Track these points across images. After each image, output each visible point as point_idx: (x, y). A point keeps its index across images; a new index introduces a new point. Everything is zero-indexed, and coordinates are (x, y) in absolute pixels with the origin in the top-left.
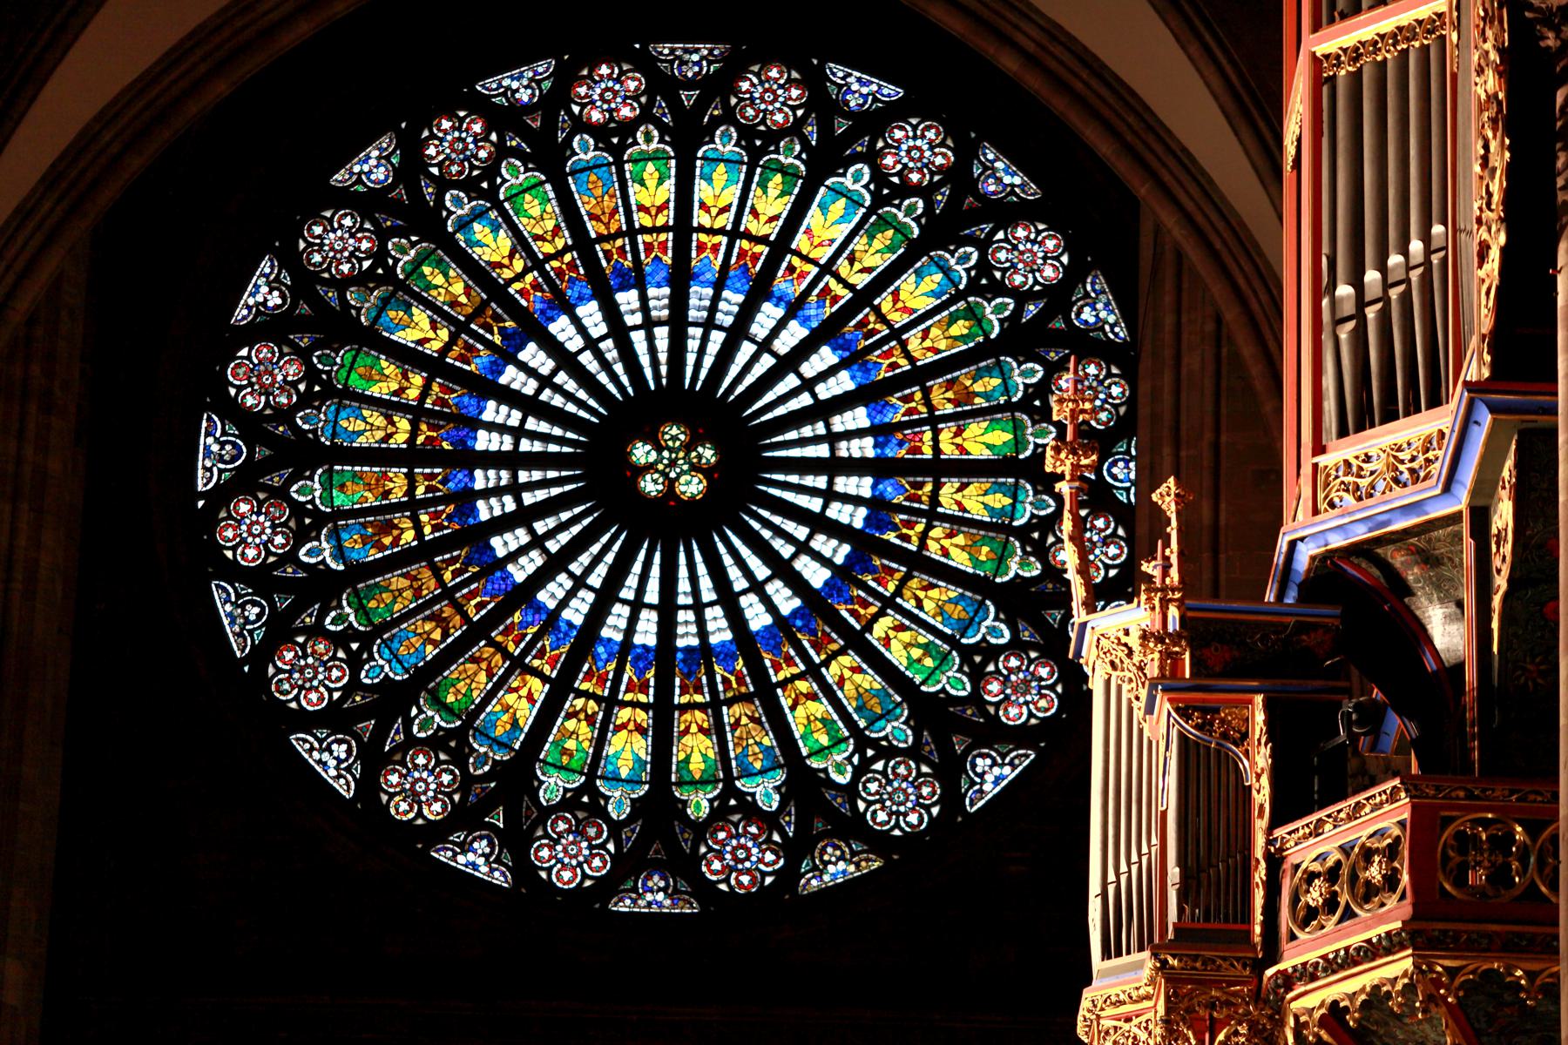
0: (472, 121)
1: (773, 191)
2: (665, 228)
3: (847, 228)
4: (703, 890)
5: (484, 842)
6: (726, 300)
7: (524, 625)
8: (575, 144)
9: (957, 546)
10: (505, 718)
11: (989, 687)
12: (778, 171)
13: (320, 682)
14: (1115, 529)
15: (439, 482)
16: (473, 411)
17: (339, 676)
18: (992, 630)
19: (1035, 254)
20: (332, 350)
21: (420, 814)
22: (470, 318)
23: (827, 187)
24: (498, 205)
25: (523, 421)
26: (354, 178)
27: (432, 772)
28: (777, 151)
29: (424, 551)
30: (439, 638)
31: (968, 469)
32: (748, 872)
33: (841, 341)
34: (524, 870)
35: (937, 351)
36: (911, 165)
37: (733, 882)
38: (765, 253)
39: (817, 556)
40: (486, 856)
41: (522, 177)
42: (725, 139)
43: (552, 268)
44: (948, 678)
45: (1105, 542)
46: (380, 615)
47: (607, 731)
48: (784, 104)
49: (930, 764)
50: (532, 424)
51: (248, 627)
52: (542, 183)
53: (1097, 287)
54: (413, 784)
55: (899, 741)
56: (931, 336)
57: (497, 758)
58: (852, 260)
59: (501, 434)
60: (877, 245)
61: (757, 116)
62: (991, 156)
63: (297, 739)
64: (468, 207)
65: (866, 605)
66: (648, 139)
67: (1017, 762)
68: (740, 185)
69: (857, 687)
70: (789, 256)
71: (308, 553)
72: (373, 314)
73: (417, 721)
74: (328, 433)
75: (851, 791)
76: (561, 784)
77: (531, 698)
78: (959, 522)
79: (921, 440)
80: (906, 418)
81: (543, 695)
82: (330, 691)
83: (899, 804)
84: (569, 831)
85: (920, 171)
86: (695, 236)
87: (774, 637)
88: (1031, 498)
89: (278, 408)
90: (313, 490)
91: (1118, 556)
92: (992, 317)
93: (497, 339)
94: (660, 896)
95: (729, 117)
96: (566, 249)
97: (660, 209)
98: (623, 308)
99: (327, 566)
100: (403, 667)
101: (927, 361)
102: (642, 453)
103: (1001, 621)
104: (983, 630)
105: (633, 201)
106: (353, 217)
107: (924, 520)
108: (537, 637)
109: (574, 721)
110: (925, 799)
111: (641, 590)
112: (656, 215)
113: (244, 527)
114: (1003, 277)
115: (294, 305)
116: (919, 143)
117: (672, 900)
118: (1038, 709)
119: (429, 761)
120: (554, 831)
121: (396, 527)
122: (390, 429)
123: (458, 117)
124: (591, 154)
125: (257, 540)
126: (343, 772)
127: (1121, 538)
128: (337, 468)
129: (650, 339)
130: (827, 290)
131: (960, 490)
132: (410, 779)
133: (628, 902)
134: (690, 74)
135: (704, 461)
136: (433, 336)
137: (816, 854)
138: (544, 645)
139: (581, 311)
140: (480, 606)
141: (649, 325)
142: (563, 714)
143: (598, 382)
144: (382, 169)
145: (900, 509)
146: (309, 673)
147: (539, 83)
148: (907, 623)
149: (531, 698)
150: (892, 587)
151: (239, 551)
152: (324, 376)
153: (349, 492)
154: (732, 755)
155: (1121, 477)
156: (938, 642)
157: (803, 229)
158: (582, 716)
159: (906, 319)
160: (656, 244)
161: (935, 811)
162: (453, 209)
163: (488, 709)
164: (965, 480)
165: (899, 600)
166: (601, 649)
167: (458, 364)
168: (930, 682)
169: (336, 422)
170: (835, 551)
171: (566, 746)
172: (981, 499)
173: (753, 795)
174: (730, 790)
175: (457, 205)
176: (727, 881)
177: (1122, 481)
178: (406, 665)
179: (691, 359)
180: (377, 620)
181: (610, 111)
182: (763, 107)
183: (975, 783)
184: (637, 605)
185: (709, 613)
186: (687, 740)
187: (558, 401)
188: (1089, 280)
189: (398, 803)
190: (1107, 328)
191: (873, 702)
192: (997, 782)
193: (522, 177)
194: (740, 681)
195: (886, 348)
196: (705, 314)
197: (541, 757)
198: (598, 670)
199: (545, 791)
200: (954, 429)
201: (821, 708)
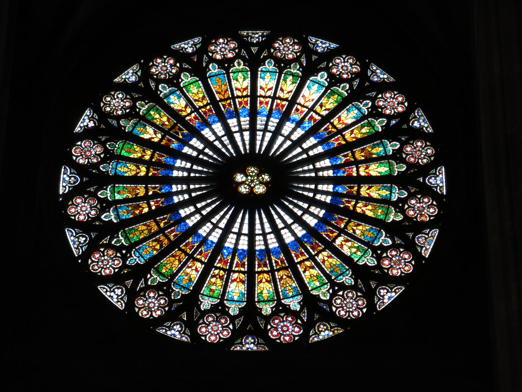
0: (169, 59)
2: (247, 96)
3: (319, 95)
5: (179, 326)
6: (272, 121)
9: (368, 210)
10: (186, 278)
11: (384, 262)
12: (291, 75)
13: (110, 266)
15: (159, 190)
17: (119, 264)
18: (384, 241)
19: (394, 103)
20: (114, 142)
21: (151, 315)
22: (170, 129)
23: (310, 80)
24: (181, 89)
26: (123, 80)
28: (290, 68)
29: (152, 215)
30: (159, 248)
31: (371, 180)
32: (288, 335)
33: (318, 135)
34: (195, 336)
36: (343, 72)
37: (282, 340)
38: (287, 104)
40: (180, 332)
42: (270, 64)
43: (202, 111)
44: (367, 259)
45: (429, 207)
47: (228, 282)
48: (292, 51)
50: (195, 167)
52: (197, 81)
54: (149, 304)
56: (354, 133)
57: (183, 293)
58: (321, 106)
59: (183, 172)
60: (331, 100)
61: (282, 56)
62: (375, 68)
63: (101, 288)
65: (332, 232)
66: (239, 64)
67: (397, 291)
68: (276, 80)
72: (131, 129)
73: (150, 280)
75: (329, 303)
77: (196, 270)
78: (369, 200)
79: (352, 171)
81: (202, 269)
82: (114, 269)
83: (349, 308)
84: (213, 321)
85: (347, 74)
88: (397, 191)
91: (434, 212)
92: (378, 125)
93: (181, 137)
95: (271, 56)
96: (208, 104)
97: (244, 89)
98: (231, 125)
100: (144, 259)
102: (239, 178)
103: (388, 237)
104: (381, 241)
106: (122, 94)
107: (355, 200)
108: (199, 247)
109: (215, 278)
110: (360, 306)
111: (241, 228)
112: (243, 92)
113: (79, 208)
114: (382, 111)
116: (346, 64)
117: (257, 347)
119: (155, 295)
120: (207, 321)
121: (141, 207)
122: (138, 171)
124: (217, 70)
125: (84, 213)
127: (435, 205)
128: (117, 185)
129: (242, 136)
130: (311, 117)
131: (368, 189)
135: (265, 180)
136: (155, 136)
137: (316, 328)
138: (202, 250)
139: (214, 126)
141: (241, 131)
142: (210, 276)
144: (134, 77)
146: (105, 262)
148: (350, 239)
149: (196, 270)
150: (342, 226)
153: (122, 194)
154: (280, 290)
155: (433, 183)
156: (362, 245)
157: (301, 95)
158: (218, 277)
160: (243, 102)
162: (163, 91)
163: (180, 274)
164: (370, 185)
166: (225, 251)
168: (360, 261)
169: (116, 169)
172: (377, 192)
173: (289, 305)
175: (164, 90)
176: (279, 339)
178: (145, 258)
181: (224, 55)
182: (284, 52)
183: (381, 299)
184: (239, 234)
185: (269, 237)
186: (261, 285)
187: (205, 158)
188: (416, 111)
189: (142, 311)
190: (424, 129)
191: (337, 269)
192: (389, 298)
194: (282, 262)
195: (336, 137)
196: (263, 127)
199: (203, 305)
200: (365, 167)
201: (315, 272)
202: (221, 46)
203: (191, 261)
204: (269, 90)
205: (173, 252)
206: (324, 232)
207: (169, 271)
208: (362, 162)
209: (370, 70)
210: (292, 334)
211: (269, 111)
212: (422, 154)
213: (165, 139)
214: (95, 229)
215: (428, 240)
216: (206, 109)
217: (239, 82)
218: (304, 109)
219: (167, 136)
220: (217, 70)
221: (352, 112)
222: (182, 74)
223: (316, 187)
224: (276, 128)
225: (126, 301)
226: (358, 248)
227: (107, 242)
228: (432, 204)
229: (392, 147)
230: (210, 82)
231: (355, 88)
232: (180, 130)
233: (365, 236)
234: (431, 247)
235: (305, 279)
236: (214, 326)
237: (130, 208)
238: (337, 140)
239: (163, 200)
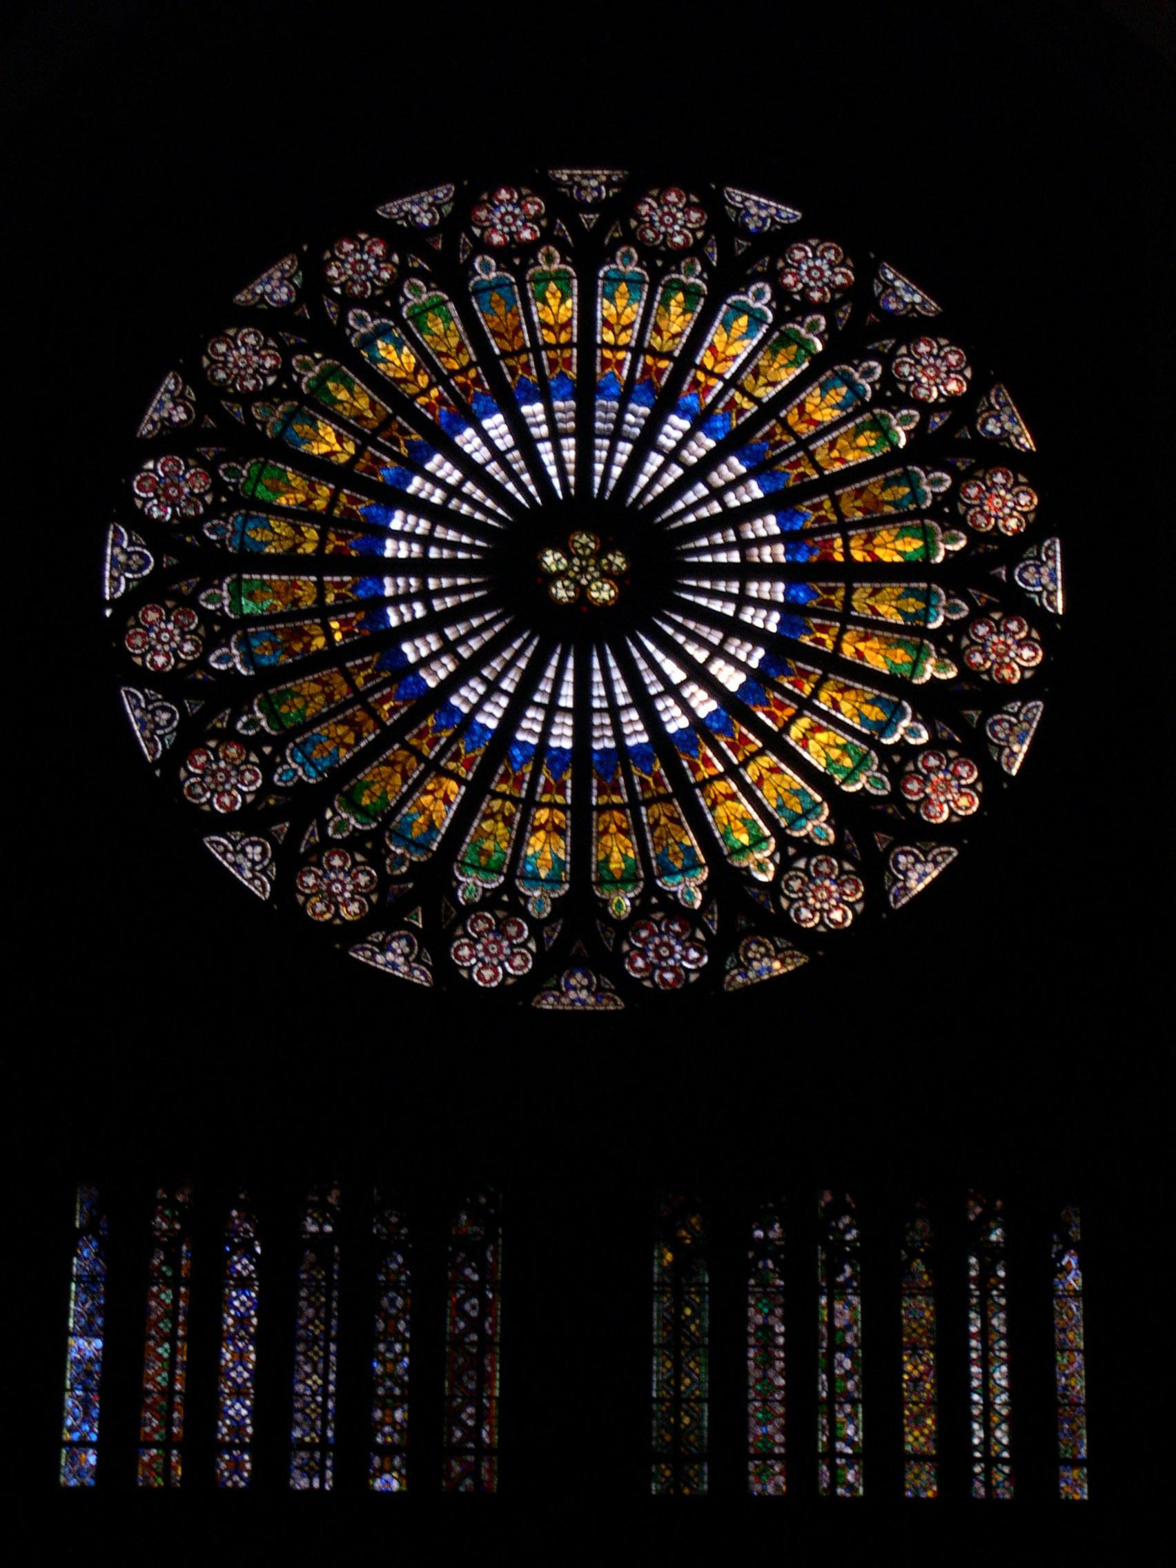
0: (374, 244)
2: (569, 345)
4: (627, 987)
7: (438, 729)
8: (477, 266)
9: (871, 649)
10: (421, 820)
14: (1029, 633)
15: (351, 590)
16: (382, 523)
17: (252, 783)
18: (910, 731)
21: (337, 914)
22: (376, 432)
24: (401, 323)
25: (432, 530)
26: (257, 298)
27: (348, 874)
28: (678, 271)
29: (333, 656)
32: (672, 969)
33: (747, 452)
34: (445, 969)
37: (657, 979)
40: (406, 956)
41: (424, 296)
42: (626, 260)
45: (1020, 644)
46: (292, 720)
49: (852, 862)
50: (439, 532)
51: (159, 732)
52: (444, 302)
53: (1001, 400)
56: (838, 446)
57: (414, 859)
58: (756, 373)
59: (409, 543)
60: (781, 359)
63: (211, 842)
64: (371, 325)
65: (782, 706)
66: (550, 259)
67: (939, 859)
68: (643, 304)
71: (219, 660)
72: (279, 429)
73: (332, 824)
74: (237, 542)
76: (479, 883)
77: (447, 801)
84: (489, 930)
85: (821, 290)
86: (599, 352)
88: (944, 603)
89: (184, 519)
90: (221, 598)
91: (1033, 658)
93: (404, 451)
94: (584, 994)
95: (630, 238)
96: (471, 365)
98: (530, 420)
99: (238, 672)
102: (551, 560)
104: (901, 731)
105: (536, 319)
106: (256, 335)
108: (451, 740)
113: (153, 635)
114: (908, 389)
115: (200, 419)
116: (818, 263)
119: (345, 862)
120: (473, 930)
121: (307, 634)
122: (298, 539)
123: (360, 240)
124: (493, 275)
128: (246, 576)
129: (557, 450)
130: (732, 402)
131: (872, 595)
132: (325, 880)
133: (551, 999)
134: (589, 199)
135: (615, 568)
137: (741, 951)
138: (459, 749)
139: (486, 423)
140: (393, 711)
141: (555, 437)
142: (479, 815)
143: (508, 492)
144: (285, 290)
146: (221, 777)
147: (439, 207)
148: (824, 724)
149: (447, 801)
150: (808, 689)
151: (148, 657)
152: (231, 488)
154: (652, 854)
155: (1033, 581)
156: (856, 742)
157: (706, 345)
158: (499, 817)
160: (560, 360)
162: (356, 327)
163: (405, 810)
166: (516, 752)
169: (243, 533)
170: (749, 655)
172: (894, 603)
173: (675, 893)
174: (651, 888)
175: (360, 322)
176: (651, 978)
177: (1033, 586)
180: (289, 724)
181: (511, 233)
182: (663, 229)
184: (552, 709)
186: (608, 840)
187: (465, 509)
188: (993, 393)
190: (1013, 439)
193: (424, 296)
194: (658, 780)
195: (793, 458)
196: (611, 426)
198: (514, 771)
200: (864, 537)
202: (503, 210)
206: (762, 704)
208: (856, 525)
211: (624, 387)
214: (196, 690)
215: (1016, 729)
216: (467, 377)
218: (712, 382)
219: (370, 448)
223: (743, 588)
224: (644, 429)
226: (843, 748)
230: (476, 306)
232: (404, 432)
235: (713, 827)
239: (362, 615)
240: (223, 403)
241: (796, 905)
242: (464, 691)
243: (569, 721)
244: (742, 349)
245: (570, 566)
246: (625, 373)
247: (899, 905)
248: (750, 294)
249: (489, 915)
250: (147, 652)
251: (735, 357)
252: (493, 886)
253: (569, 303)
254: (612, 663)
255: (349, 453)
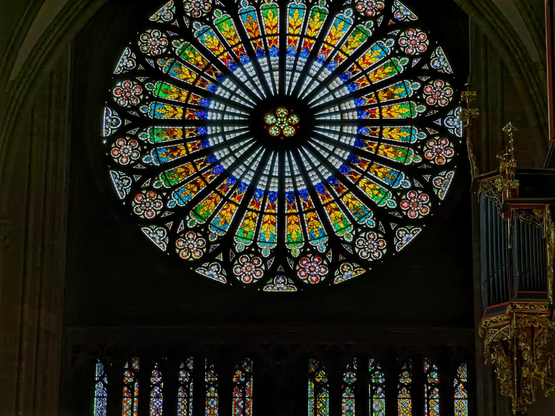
1: (316, 20)
2: (276, 34)
3: (344, 33)
5: (216, 266)
9: (390, 152)
10: (222, 220)
11: (403, 205)
12: (318, 12)
13: (152, 208)
14: (449, 144)
16: (206, 105)
17: (159, 205)
18: (404, 183)
19: (416, 41)
21: (191, 257)
22: (204, 70)
23: (337, 17)
24: (213, 27)
25: (225, 108)
26: (159, 18)
29: (190, 158)
30: (196, 190)
31: (393, 122)
32: (315, 275)
34: (231, 277)
35: (380, 79)
36: (368, 8)
37: (309, 280)
38: (314, 43)
39: (337, 157)
41: (222, 16)
43: (234, 50)
46: (174, 182)
52: (229, 18)
53: (440, 53)
54: (188, 245)
55: (370, 225)
56: (378, 73)
58: (347, 45)
59: (217, 113)
60: (356, 39)
62: (398, 4)
63: (144, 229)
64: (202, 28)
65: (356, 174)
67: (415, 232)
69: (354, 205)
70: (323, 44)
72: (167, 69)
73: (189, 222)
75: (353, 245)
76: (244, 244)
77: (232, 213)
79: (375, 112)
80: (369, 104)
81: (236, 211)
82: (156, 211)
83: (371, 249)
84: (247, 262)
85: (372, 10)
86: (287, 37)
87: (322, 187)
88: (417, 133)
90: (147, 136)
92: (401, 65)
93: (214, 77)
94: (282, 285)
96: (239, 43)
97: (274, 27)
98: (261, 65)
100: (183, 202)
101: (376, 82)
102: (270, 119)
103: (407, 179)
104: (401, 183)
105: (264, 24)
106: (158, 32)
107: (377, 142)
108: (233, 189)
109: (248, 220)
110: (380, 247)
112: (273, 30)
113: (121, 150)
115: (137, 66)
118: (422, 213)
121: (178, 149)
122: (175, 112)
124: (247, 7)
126: (162, 242)
128: (156, 127)
129: (272, 76)
130: (338, 56)
133: (270, 288)
135: (293, 122)
137: (340, 269)
138: (236, 192)
139: (245, 66)
140: (211, 178)
141: (271, 71)
142: (244, 218)
144: (169, 14)
145: (368, 138)
146: (148, 205)
148: (372, 181)
149: (231, 213)
150: (366, 167)
151: (120, 159)
153: (161, 136)
154: (308, 232)
155: (451, 124)
156: (384, 188)
157: (328, 33)
158: (251, 218)
159: (368, 66)
160: (273, 40)
161: (385, 251)
163: (216, 216)
164: (392, 127)
165: (368, 173)
166: (257, 193)
167: (200, 87)
169: (155, 110)
170: (344, 154)
171: (245, 230)
172: (398, 134)
173: (316, 247)
174: (307, 245)
175: (197, 27)
176: (307, 279)
177: (451, 126)
178: (184, 201)
179: (287, 83)
180: (172, 184)
183: (400, 241)
184: (270, 176)
187: (238, 100)
188: (437, 50)
189: (182, 253)
190: (444, 68)
191: (360, 211)
192: (407, 240)
193: (222, 16)
194: (310, 204)
195: (361, 78)
196: (292, 66)
197: (236, 234)
198: (256, 201)
200: (387, 108)
201: (340, 213)
203: (226, 203)
204: (297, 27)
205: (209, 195)
206: (349, 174)
207: (206, 213)
209: (394, 6)
210: (318, 274)
211: (297, 51)
212: (441, 95)
213: (200, 79)
217: (269, 20)
218: (330, 48)
219: (201, 76)
220: (247, 7)
221: (376, 51)
222: (215, 11)
223: (341, 129)
225: (167, 243)
227: (149, 184)
228: (449, 146)
229: (413, 87)
231: (379, 26)
232: (214, 70)
233: (386, 178)
234: (447, 189)
235: (330, 221)
236: (248, 266)
237: (169, 150)
238: (361, 80)
239: (199, 142)
240: (146, 59)
241: (361, 251)
242: (237, 170)
243: (277, 181)
244: (342, 35)
245: (277, 121)
246: (297, 45)
247: (400, 250)
248: (345, 13)
249: (247, 256)
250: (119, 157)
251: (339, 38)
252: (249, 245)
253: (276, 18)
254: (293, 158)
255: (193, 78)
